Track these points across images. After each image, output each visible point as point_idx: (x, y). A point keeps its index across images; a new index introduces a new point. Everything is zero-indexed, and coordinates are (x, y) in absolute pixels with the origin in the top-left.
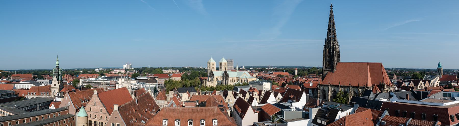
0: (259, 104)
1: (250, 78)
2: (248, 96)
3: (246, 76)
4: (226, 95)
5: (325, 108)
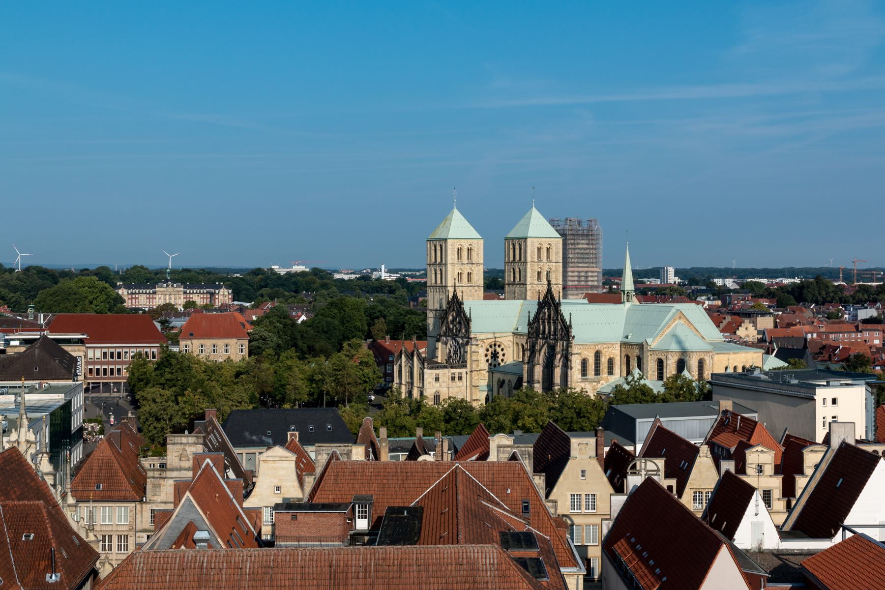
0: (784, 535)
1: (717, 348)
2: (704, 475)
4: (552, 461)
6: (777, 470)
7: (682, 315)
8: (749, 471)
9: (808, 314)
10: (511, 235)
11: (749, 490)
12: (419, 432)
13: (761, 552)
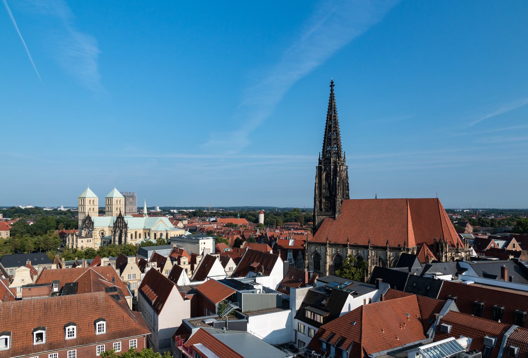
0: (191, 281)
1: (172, 230)
2: (169, 266)
3: (163, 226)
4: (122, 265)
5: (319, 289)
6: (189, 263)
7: (161, 220)
8: (181, 264)
9: (197, 220)
10: (107, 196)
11: (182, 269)
12: (76, 259)
13: (185, 286)
